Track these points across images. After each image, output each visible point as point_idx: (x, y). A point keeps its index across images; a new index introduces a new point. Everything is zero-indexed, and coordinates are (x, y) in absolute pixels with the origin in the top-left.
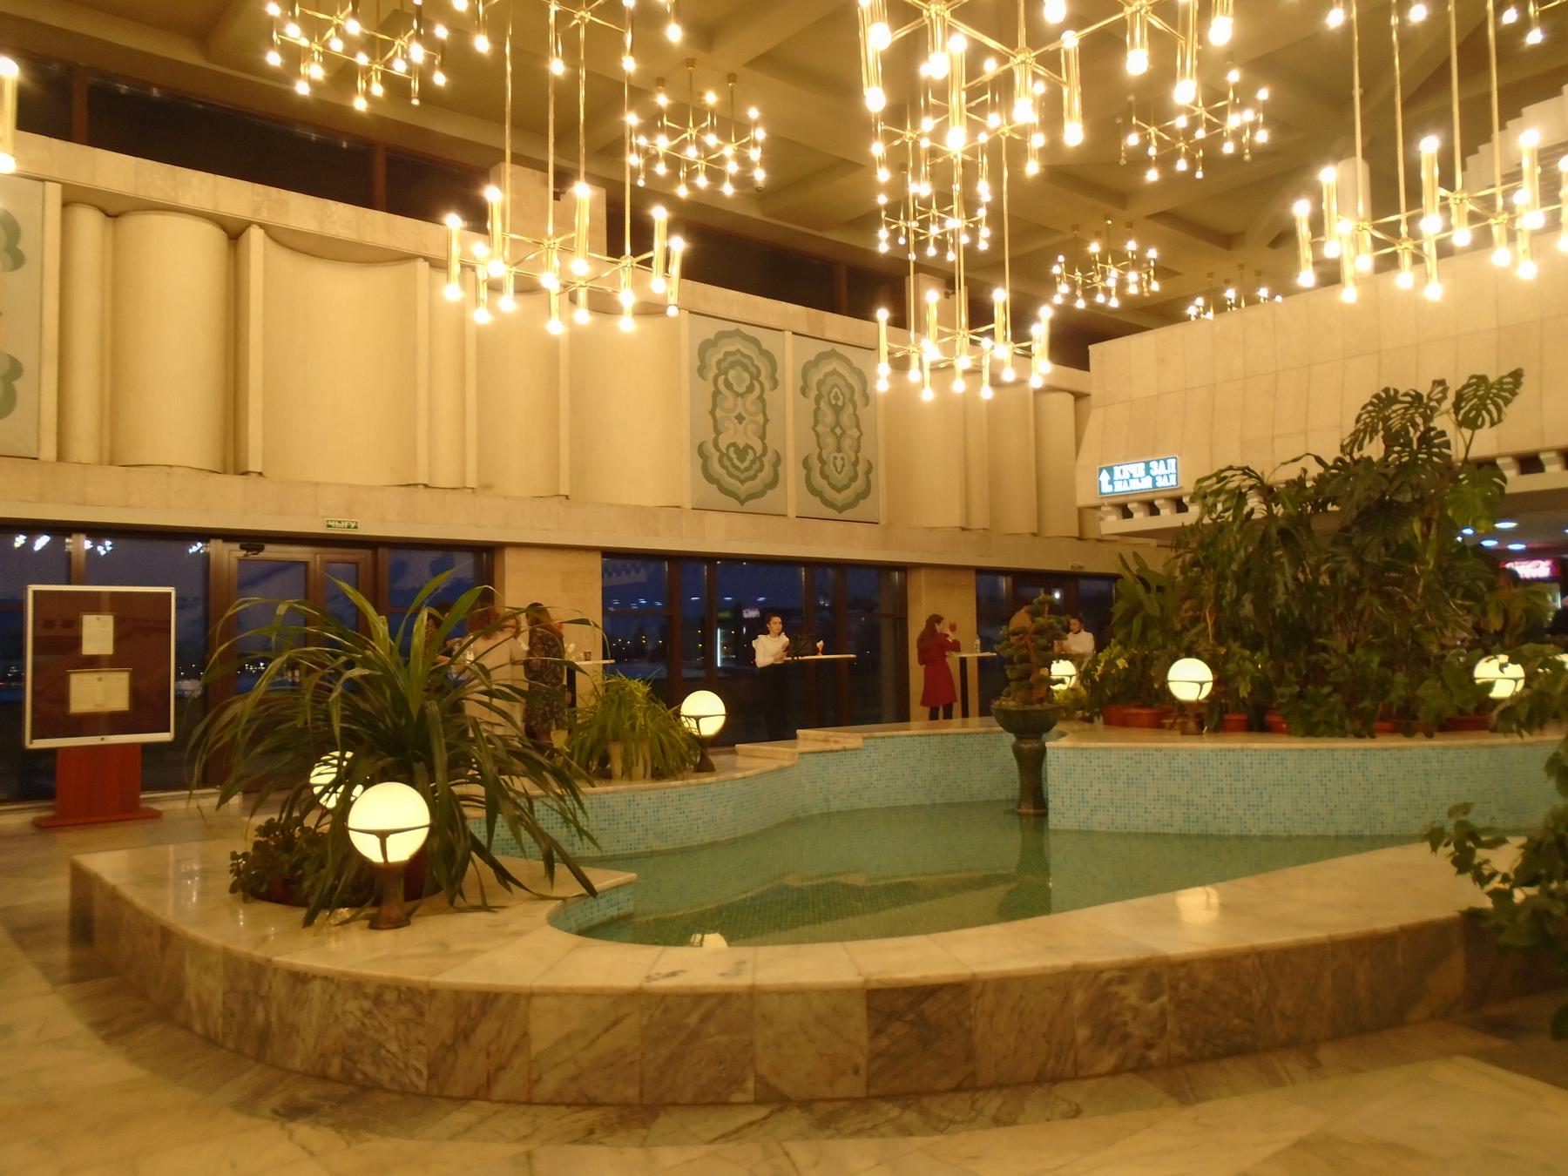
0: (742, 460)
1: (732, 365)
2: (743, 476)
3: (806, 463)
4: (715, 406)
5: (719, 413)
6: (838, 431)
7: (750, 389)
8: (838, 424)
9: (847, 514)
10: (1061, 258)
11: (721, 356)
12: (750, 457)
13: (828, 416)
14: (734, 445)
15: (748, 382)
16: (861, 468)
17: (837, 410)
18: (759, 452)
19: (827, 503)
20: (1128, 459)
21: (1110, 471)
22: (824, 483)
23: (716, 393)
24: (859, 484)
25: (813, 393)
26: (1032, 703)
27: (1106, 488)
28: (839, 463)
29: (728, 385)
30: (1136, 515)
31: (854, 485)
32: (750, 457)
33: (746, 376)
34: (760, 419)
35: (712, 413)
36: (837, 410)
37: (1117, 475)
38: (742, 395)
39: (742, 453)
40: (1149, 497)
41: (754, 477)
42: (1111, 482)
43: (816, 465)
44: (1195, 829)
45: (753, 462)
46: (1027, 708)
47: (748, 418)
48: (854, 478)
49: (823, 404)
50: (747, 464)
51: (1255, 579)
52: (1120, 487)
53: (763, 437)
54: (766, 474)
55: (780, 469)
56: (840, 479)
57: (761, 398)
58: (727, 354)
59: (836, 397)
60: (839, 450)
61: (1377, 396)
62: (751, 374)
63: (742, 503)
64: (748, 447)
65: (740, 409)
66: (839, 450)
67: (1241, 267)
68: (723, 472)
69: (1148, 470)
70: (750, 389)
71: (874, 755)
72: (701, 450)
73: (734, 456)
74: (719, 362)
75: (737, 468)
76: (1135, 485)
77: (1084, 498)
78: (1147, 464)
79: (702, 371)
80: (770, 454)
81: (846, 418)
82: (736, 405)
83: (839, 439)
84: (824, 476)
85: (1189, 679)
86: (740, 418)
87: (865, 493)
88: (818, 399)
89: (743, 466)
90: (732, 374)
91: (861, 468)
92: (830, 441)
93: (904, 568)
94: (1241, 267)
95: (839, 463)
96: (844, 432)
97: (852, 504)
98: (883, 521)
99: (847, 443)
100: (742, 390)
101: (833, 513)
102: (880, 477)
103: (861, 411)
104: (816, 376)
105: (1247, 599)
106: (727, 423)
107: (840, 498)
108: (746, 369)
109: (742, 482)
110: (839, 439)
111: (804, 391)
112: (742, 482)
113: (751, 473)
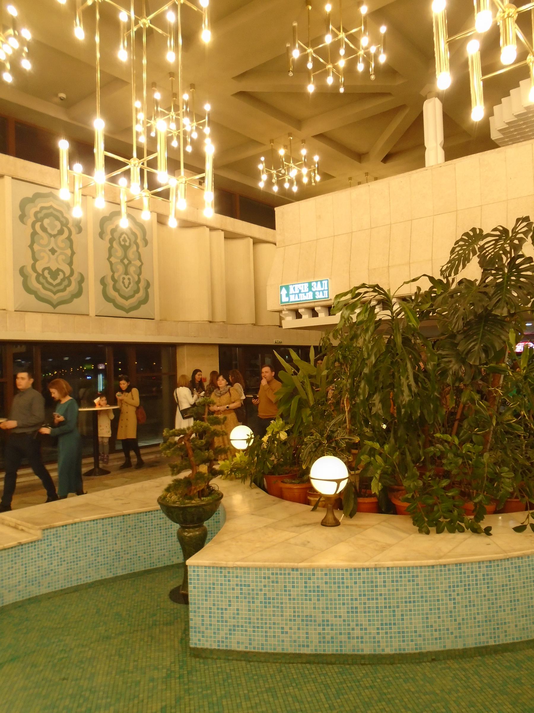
0: (55, 279)
1: (47, 216)
2: (55, 289)
3: (103, 281)
4: (33, 242)
5: (36, 247)
6: (126, 262)
7: (61, 232)
8: (126, 256)
9: (132, 314)
10: (263, 159)
11: (38, 209)
12: (61, 276)
13: (119, 252)
14: (48, 268)
15: (59, 227)
16: (142, 285)
17: (125, 248)
18: (67, 274)
20: (298, 280)
21: (287, 288)
22: (116, 294)
23: (34, 234)
24: (141, 294)
25: (108, 237)
26: (191, 498)
27: (285, 299)
28: (126, 282)
29: (44, 229)
30: (303, 317)
31: (137, 296)
32: (61, 276)
33: (58, 224)
34: (69, 252)
35: (31, 247)
36: (125, 248)
37: (291, 291)
38: (55, 236)
39: (54, 274)
40: (312, 305)
41: (64, 290)
42: (288, 295)
43: (110, 283)
44: (330, 649)
45: (63, 280)
46: (188, 503)
47: (59, 251)
48: (137, 291)
49: (115, 244)
50: (58, 281)
51: (384, 381)
52: (293, 298)
53: (71, 264)
54: (73, 288)
55: (83, 285)
56: (127, 291)
57: (69, 239)
58: (42, 208)
59: (125, 240)
60: (126, 273)
61: (466, 234)
62: (61, 222)
63: (55, 306)
64: (58, 270)
65: (53, 245)
66: (126, 273)
67: (367, 174)
68: (40, 286)
69: (310, 287)
70: (61, 232)
71: (55, 543)
72: (22, 271)
73: (48, 276)
74: (36, 214)
75: (51, 284)
76: (303, 297)
77: (272, 304)
78: (310, 284)
79: (22, 218)
80: (76, 275)
81: (131, 253)
82: (49, 242)
83: (126, 267)
84: (115, 289)
85: (329, 473)
86: (53, 251)
87: (145, 300)
88: (111, 241)
89: (55, 283)
90: (46, 222)
91: (142, 285)
92: (120, 268)
93: (174, 346)
94: (367, 174)
95: (126, 282)
96: (130, 262)
97: (136, 307)
98: (157, 318)
99: (132, 269)
100: (55, 232)
101: (123, 313)
102: (155, 291)
103: (141, 249)
105: (376, 398)
106: (42, 254)
107: (127, 303)
108: (57, 219)
109: (55, 293)
110: (126, 267)
111: (101, 235)
112: (55, 293)
113: (62, 287)
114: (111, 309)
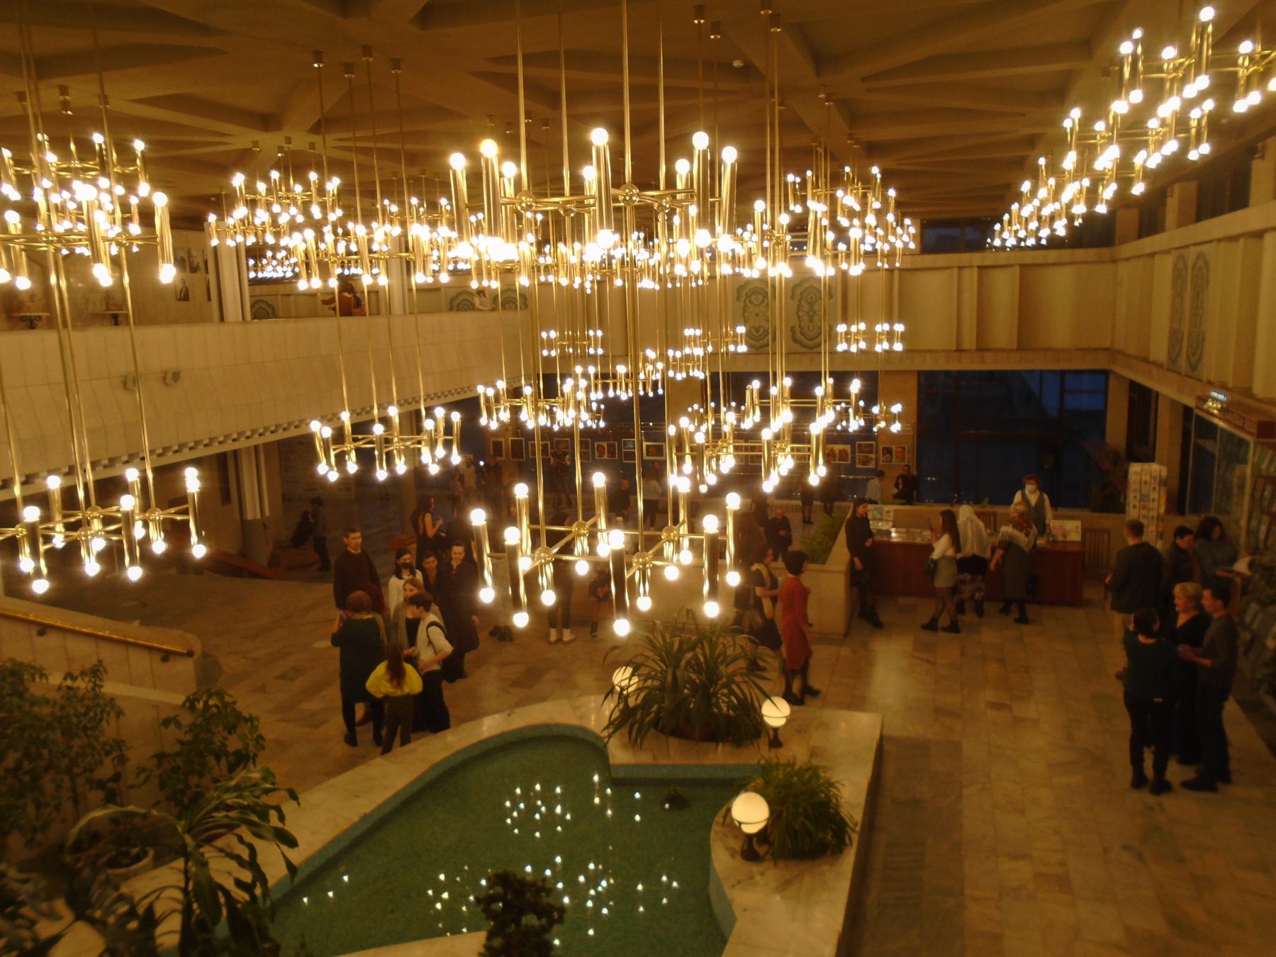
3: (792, 330)
7: (762, 302)
13: (806, 307)
17: (811, 304)
19: (802, 344)
23: (745, 306)
25: (798, 297)
60: (811, 321)
66: (811, 321)
70: (762, 302)
79: (738, 299)
86: (757, 315)
88: (800, 301)
90: (753, 298)
92: (806, 318)
104: (798, 291)
114: (798, 348)
